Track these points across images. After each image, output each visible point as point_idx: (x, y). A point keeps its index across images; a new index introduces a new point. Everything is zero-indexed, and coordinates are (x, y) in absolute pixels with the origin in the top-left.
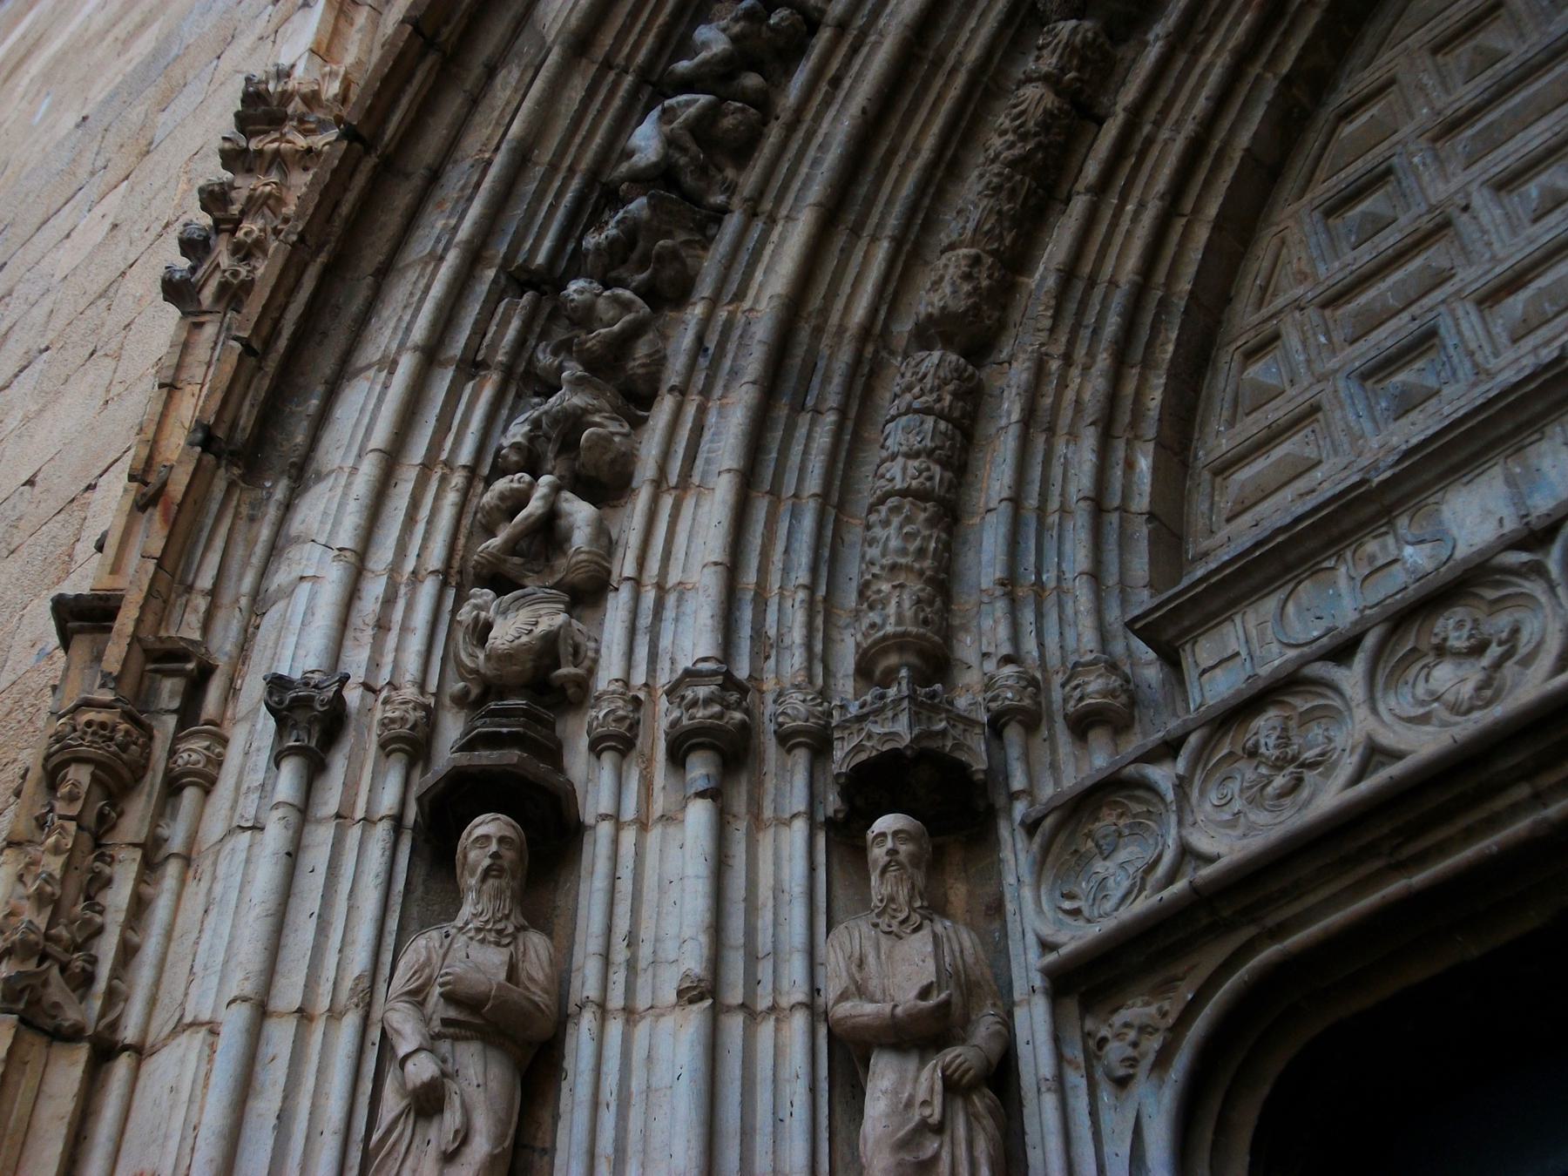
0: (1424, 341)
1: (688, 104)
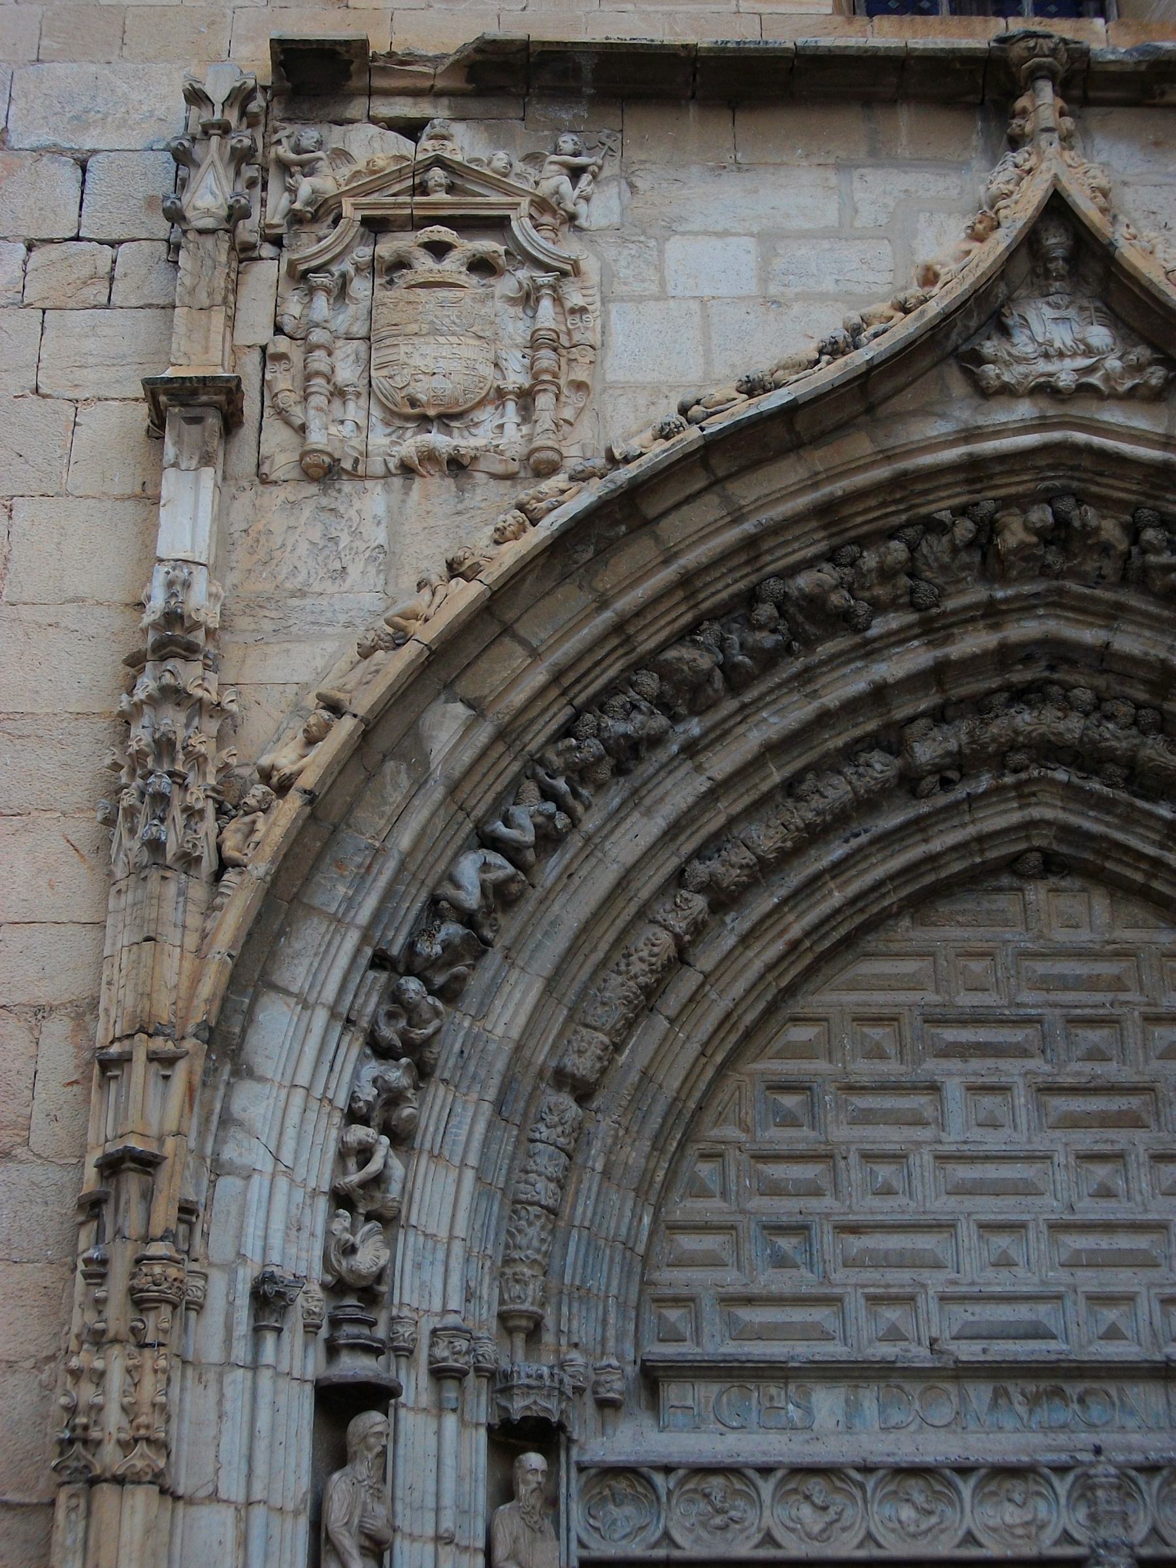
0: (801, 1229)
1: (500, 867)
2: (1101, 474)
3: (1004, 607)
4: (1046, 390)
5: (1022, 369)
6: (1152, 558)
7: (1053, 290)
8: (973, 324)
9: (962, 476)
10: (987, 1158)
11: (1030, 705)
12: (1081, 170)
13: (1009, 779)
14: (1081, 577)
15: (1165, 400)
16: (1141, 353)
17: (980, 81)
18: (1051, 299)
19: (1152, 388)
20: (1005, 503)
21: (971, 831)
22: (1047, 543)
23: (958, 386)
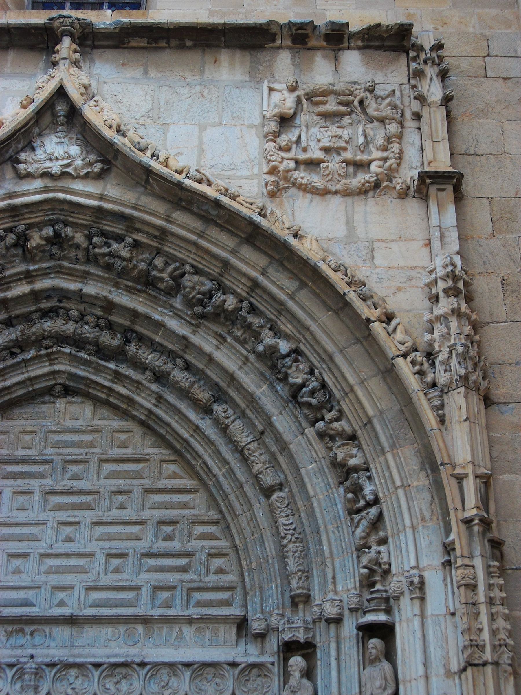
2: (73, 213)
3: (34, 274)
4: (46, 174)
5: (36, 165)
6: (97, 250)
7: (58, 130)
8: (20, 146)
9: (8, 214)
10: (17, 524)
11: (52, 319)
12: (77, 76)
13: (43, 352)
14: (69, 259)
15: (103, 178)
16: (92, 157)
17: (46, 38)
18: (57, 134)
19: (96, 173)
20: (30, 226)
21: (26, 375)
22: (53, 244)
23: (9, 174)
